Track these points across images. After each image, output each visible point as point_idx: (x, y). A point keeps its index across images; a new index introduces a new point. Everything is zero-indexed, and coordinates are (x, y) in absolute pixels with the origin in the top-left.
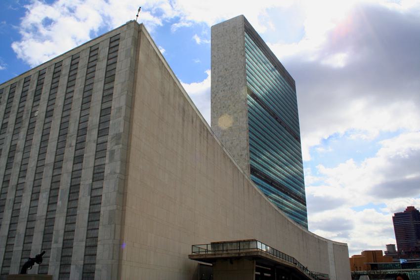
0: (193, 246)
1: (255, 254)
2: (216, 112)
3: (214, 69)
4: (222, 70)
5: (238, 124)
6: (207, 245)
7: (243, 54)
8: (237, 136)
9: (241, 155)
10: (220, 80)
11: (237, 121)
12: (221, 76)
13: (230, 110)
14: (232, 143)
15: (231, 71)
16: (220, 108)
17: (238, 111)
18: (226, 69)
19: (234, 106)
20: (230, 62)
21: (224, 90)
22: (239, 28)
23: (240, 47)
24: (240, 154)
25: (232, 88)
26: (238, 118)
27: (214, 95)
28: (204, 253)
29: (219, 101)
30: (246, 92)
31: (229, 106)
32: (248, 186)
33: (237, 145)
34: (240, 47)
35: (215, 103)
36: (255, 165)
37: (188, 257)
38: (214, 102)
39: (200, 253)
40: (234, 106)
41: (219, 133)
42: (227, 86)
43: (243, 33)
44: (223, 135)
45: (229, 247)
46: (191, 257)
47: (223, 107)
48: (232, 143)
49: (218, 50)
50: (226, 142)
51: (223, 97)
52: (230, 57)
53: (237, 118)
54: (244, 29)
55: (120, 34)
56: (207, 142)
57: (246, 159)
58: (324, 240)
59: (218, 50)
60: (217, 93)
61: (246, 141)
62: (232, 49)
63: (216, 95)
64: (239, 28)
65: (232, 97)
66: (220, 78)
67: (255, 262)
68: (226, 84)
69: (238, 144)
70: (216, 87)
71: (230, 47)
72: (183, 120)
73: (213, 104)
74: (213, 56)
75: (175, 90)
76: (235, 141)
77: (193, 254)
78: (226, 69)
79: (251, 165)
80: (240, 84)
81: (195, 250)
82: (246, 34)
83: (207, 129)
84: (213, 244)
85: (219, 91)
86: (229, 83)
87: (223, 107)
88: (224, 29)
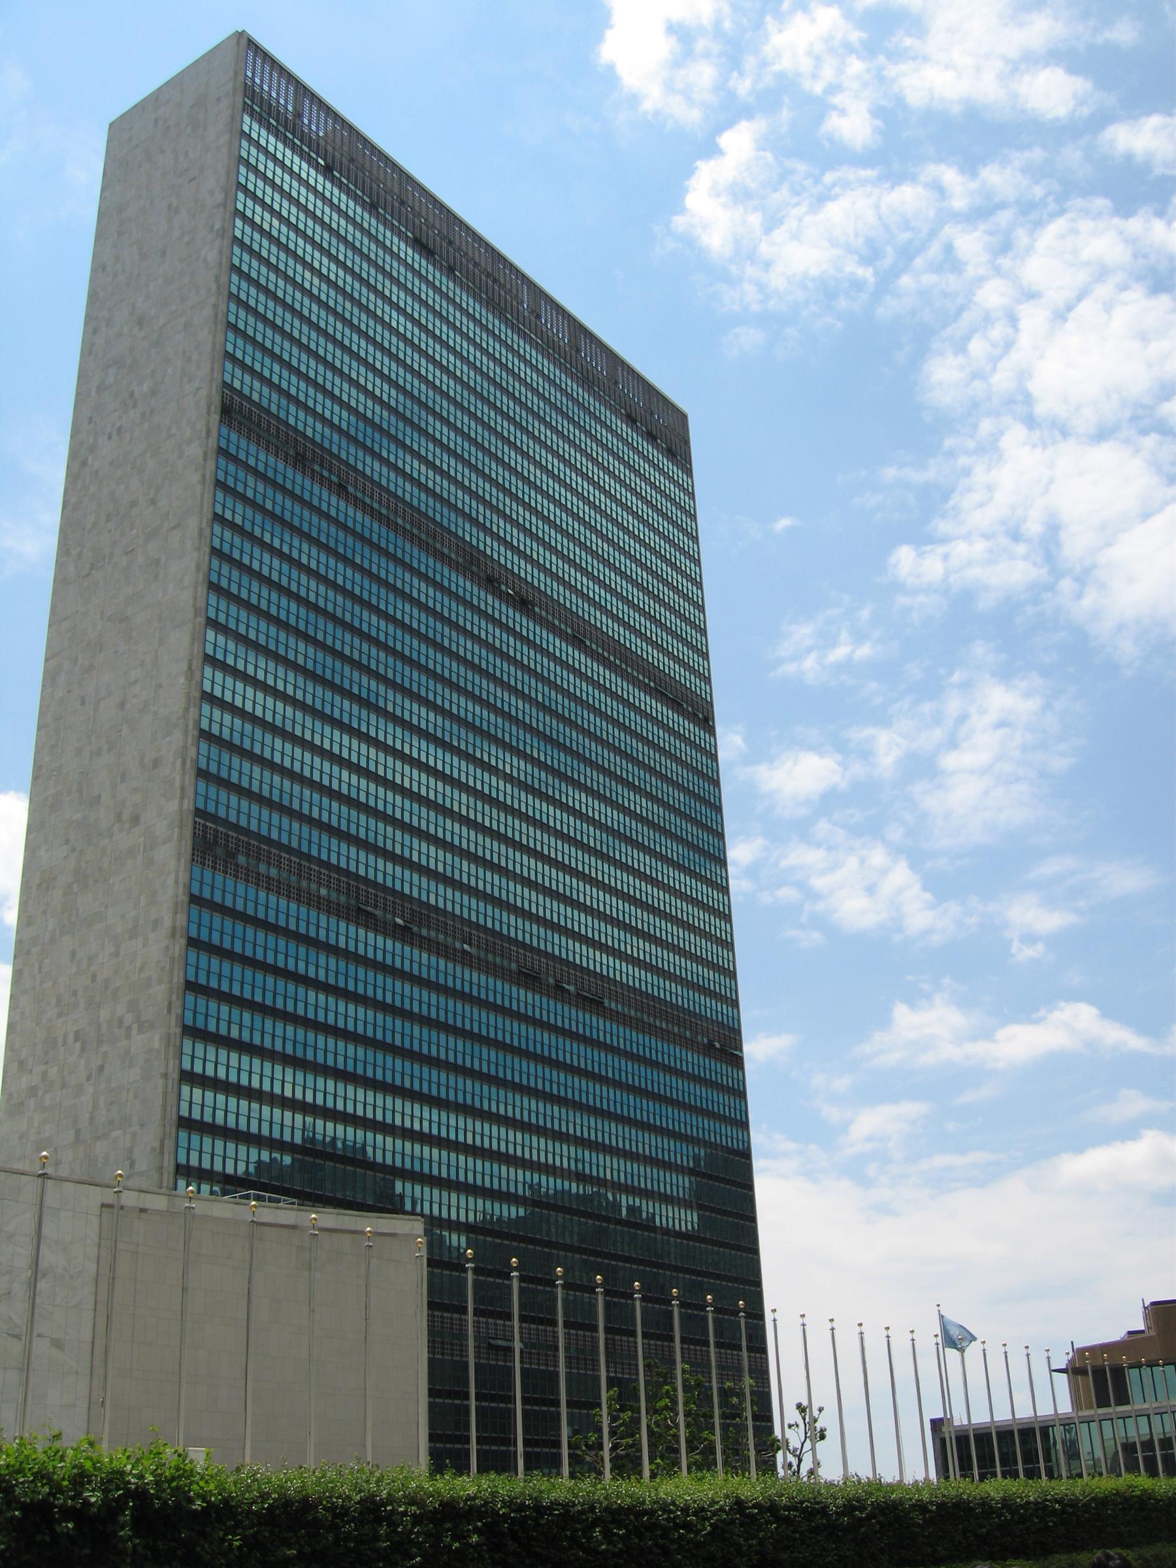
3: (95, 331)
7: (217, 226)
9: (156, 763)
14: (122, 705)
15: (161, 324)
21: (119, 430)
22: (218, 100)
23: (212, 193)
26: (163, 559)
31: (134, 504)
34: (212, 193)
40: (153, 502)
42: (135, 406)
43: (235, 121)
48: (122, 705)
51: (111, 463)
52: (164, 254)
53: (158, 561)
60: (93, 449)
61: (182, 680)
63: (84, 463)
64: (218, 100)
66: (112, 372)
68: (132, 394)
70: (90, 420)
71: (170, 206)
74: (98, 268)
78: (140, 323)
79: (198, 812)
80: (190, 381)
86: (145, 387)
88: (156, 121)
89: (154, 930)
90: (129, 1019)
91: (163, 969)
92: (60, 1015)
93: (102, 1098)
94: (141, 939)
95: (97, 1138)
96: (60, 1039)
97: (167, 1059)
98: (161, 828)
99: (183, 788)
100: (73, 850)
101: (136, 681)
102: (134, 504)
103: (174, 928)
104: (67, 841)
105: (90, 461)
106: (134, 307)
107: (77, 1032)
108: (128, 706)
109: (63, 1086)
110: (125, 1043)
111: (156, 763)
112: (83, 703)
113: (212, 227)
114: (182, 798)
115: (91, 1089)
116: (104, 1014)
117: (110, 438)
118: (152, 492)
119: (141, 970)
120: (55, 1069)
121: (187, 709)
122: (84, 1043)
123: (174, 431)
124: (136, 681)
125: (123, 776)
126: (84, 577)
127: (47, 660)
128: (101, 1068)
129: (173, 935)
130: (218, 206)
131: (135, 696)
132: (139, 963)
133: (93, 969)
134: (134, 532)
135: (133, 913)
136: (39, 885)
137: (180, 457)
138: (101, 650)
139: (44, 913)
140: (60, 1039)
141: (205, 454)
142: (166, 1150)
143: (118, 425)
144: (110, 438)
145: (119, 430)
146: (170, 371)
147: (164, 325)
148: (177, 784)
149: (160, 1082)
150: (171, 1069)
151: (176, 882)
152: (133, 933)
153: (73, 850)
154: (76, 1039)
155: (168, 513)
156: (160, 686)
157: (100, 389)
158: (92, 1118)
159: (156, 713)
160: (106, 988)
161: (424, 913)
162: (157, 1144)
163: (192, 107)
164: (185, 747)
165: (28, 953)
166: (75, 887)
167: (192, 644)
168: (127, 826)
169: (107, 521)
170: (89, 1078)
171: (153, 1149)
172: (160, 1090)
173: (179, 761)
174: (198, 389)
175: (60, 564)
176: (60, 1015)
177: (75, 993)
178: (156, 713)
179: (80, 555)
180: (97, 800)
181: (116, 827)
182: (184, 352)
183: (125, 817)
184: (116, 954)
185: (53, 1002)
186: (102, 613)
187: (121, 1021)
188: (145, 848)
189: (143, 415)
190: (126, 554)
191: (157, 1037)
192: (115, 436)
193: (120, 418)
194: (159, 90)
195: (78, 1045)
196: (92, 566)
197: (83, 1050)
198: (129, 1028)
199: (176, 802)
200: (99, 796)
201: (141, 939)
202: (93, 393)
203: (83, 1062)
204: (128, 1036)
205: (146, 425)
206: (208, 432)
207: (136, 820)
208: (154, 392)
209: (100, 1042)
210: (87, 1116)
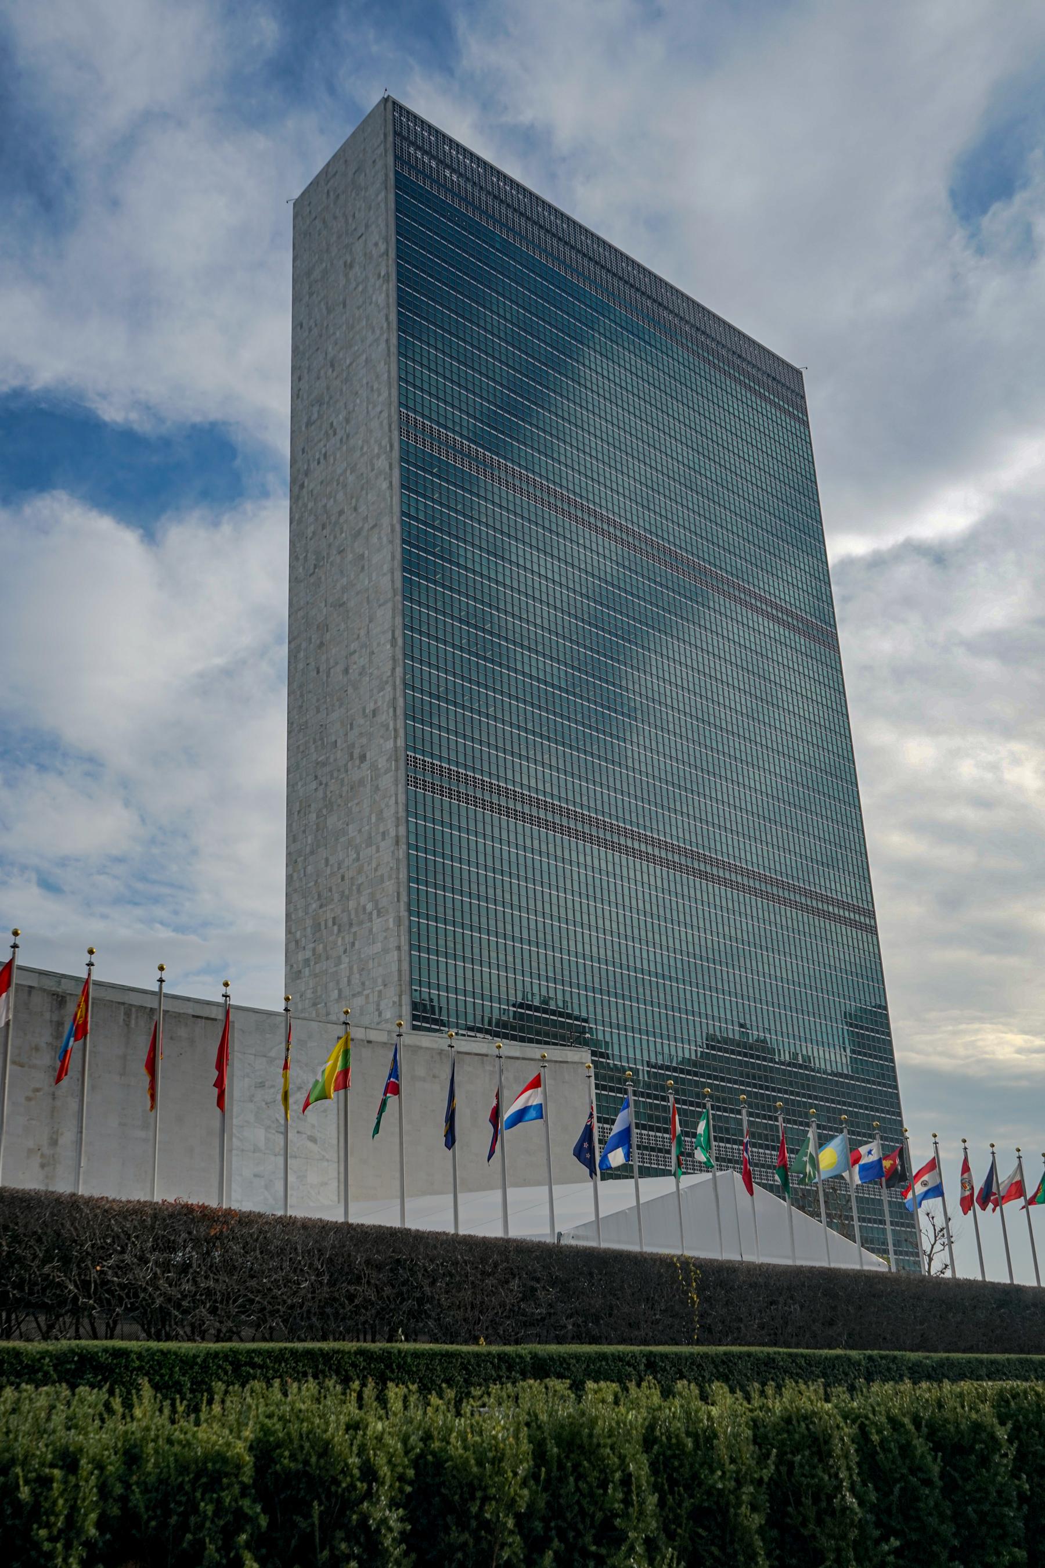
2: (301, 557)
4: (322, 372)
5: (367, 582)
8: (363, 633)
9: (374, 713)
10: (315, 416)
11: (363, 568)
12: (320, 401)
13: (341, 533)
14: (346, 671)
15: (348, 362)
16: (314, 533)
17: (366, 527)
20: (344, 327)
24: (371, 706)
25: (348, 436)
27: (296, 489)
29: (310, 505)
31: (341, 513)
33: (362, 673)
35: (300, 521)
40: (355, 509)
41: (310, 639)
42: (335, 434)
44: (322, 644)
47: (324, 527)
49: (311, 294)
50: (328, 676)
51: (322, 482)
52: (345, 306)
53: (363, 555)
57: (387, 729)
59: (311, 294)
60: (307, 473)
61: (389, 646)
62: (351, 266)
63: (302, 486)
65: (348, 472)
66: (315, 409)
68: (332, 424)
69: (363, 667)
71: (345, 263)
73: (295, 523)
76: (357, 655)
78: (332, 365)
85: (313, 465)
86: (341, 417)
89: (383, 839)
90: (369, 907)
91: (391, 869)
92: (321, 907)
93: (355, 967)
94: (374, 847)
95: (354, 995)
96: (323, 924)
97: (399, 936)
98: (382, 763)
99: (396, 730)
100: (321, 784)
101: (355, 652)
103: (397, 836)
104: (316, 777)
107: (334, 918)
109: (327, 959)
110: (369, 924)
111: (374, 713)
112: (318, 672)
114: (396, 738)
115: (347, 960)
116: (352, 904)
117: (319, 463)
118: (354, 501)
119: (376, 870)
120: (321, 946)
121: (394, 669)
122: (340, 926)
123: (365, 449)
124: (355, 652)
127: (289, 642)
128: (353, 944)
129: (397, 843)
131: (355, 663)
132: (374, 866)
133: (341, 871)
134: (343, 535)
135: (367, 828)
136: (299, 812)
137: (373, 470)
139: (304, 832)
140: (323, 924)
142: (403, 1003)
143: (323, 451)
144: (319, 463)
146: (358, 401)
147: (351, 364)
148: (391, 727)
149: (396, 953)
150: (403, 943)
151: (397, 803)
152: (369, 841)
153: (321, 784)
154: (334, 924)
156: (373, 653)
157: (309, 424)
158: (349, 981)
159: (371, 674)
160: (352, 884)
162: (396, 999)
164: (394, 698)
165: (296, 862)
166: (324, 812)
167: (394, 618)
168: (357, 762)
169: (323, 529)
170: (345, 952)
171: (394, 1003)
172: (396, 958)
173: (391, 710)
175: (292, 568)
176: (321, 907)
177: (330, 890)
178: (371, 674)
183: (356, 755)
184: (358, 859)
185: (316, 897)
187: (364, 908)
189: (341, 440)
191: (391, 920)
192: (322, 460)
193: (325, 446)
195: (336, 928)
196: (315, 567)
197: (339, 931)
198: (371, 913)
199: (392, 741)
201: (374, 847)
203: (340, 942)
204: (371, 920)
205: (345, 448)
207: (363, 758)
208: (347, 421)
209: (351, 925)
210: (346, 979)
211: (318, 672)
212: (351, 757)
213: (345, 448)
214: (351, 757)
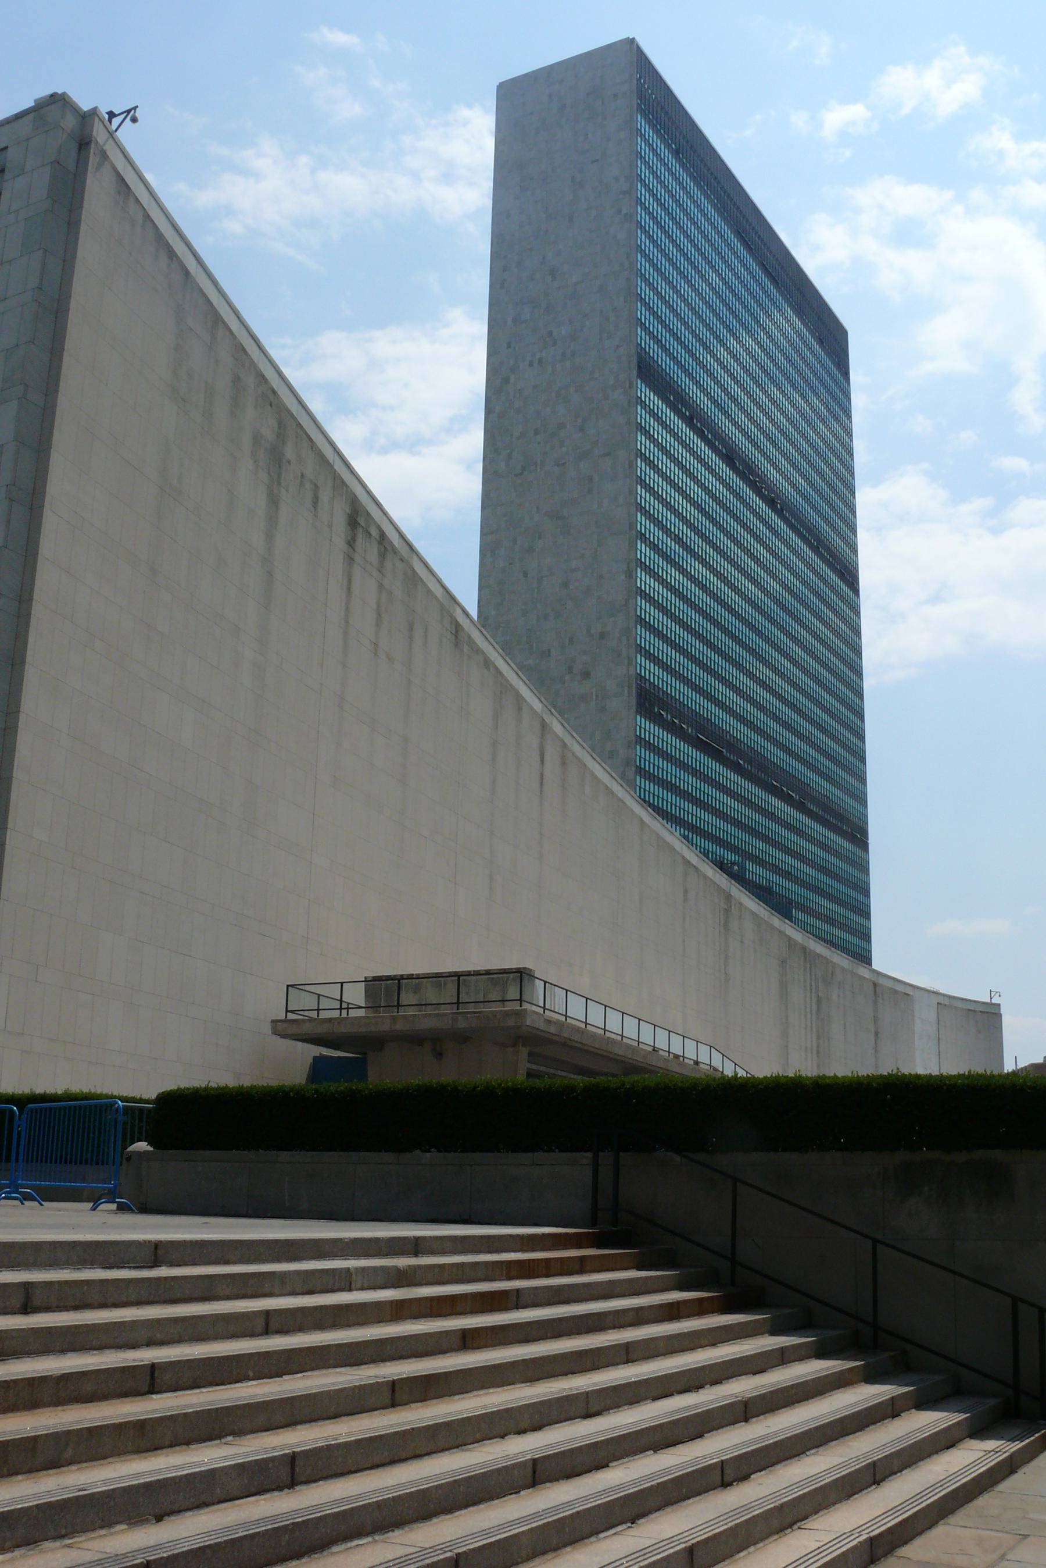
0: (288, 986)
1: (511, 1022)
3: (505, 269)
5: (595, 506)
6: (342, 983)
7: (624, 211)
9: (602, 636)
10: (528, 317)
11: (590, 491)
14: (565, 585)
18: (553, 273)
19: (581, 429)
22: (616, 95)
23: (617, 179)
28: (335, 1014)
30: (635, 372)
31: (561, 426)
32: (564, 764)
34: (617, 179)
36: (654, 674)
37: (267, 1029)
38: (498, 409)
39: (324, 1015)
40: (581, 429)
41: (515, 540)
42: (554, 344)
45: (431, 995)
46: (284, 1029)
47: (536, 432)
48: (565, 585)
51: (535, 387)
52: (571, 220)
53: (591, 479)
54: (635, 101)
55: (6, 148)
56: (381, 586)
58: (900, 988)
61: (623, 577)
63: (506, 381)
67: (524, 1052)
68: (550, 334)
70: (509, 346)
71: (573, 178)
72: (274, 501)
75: (237, 380)
77: (291, 1016)
78: (553, 273)
81: (303, 1002)
82: (641, 122)
83: (382, 535)
84: (376, 985)
87: (536, 432)
88: (550, 95)
102: (561, 426)
105: (512, 380)
106: (544, 258)
108: (571, 587)
112: (525, 575)
113: (619, 212)
117: (531, 365)
118: (580, 420)
125: (571, 641)
126: (516, 475)
130: (624, 193)
134: (564, 449)
138: (540, 538)
141: (629, 402)
143: (538, 356)
145: (540, 361)
146: (588, 323)
155: (597, 441)
156: (601, 577)
161: (733, 745)
163: (588, 94)
173: (624, 638)
174: (618, 347)
179: (510, 456)
180: (547, 654)
181: (567, 677)
182: (601, 312)
186: (538, 508)
188: (597, 696)
189: (564, 354)
190: (558, 466)
194: (552, 67)
196: (524, 469)
200: (549, 651)
202: (509, 322)
205: (568, 364)
206: (631, 384)
207: (586, 675)
211: (525, 575)
212: (570, 670)
213: (568, 364)
214: (570, 670)
